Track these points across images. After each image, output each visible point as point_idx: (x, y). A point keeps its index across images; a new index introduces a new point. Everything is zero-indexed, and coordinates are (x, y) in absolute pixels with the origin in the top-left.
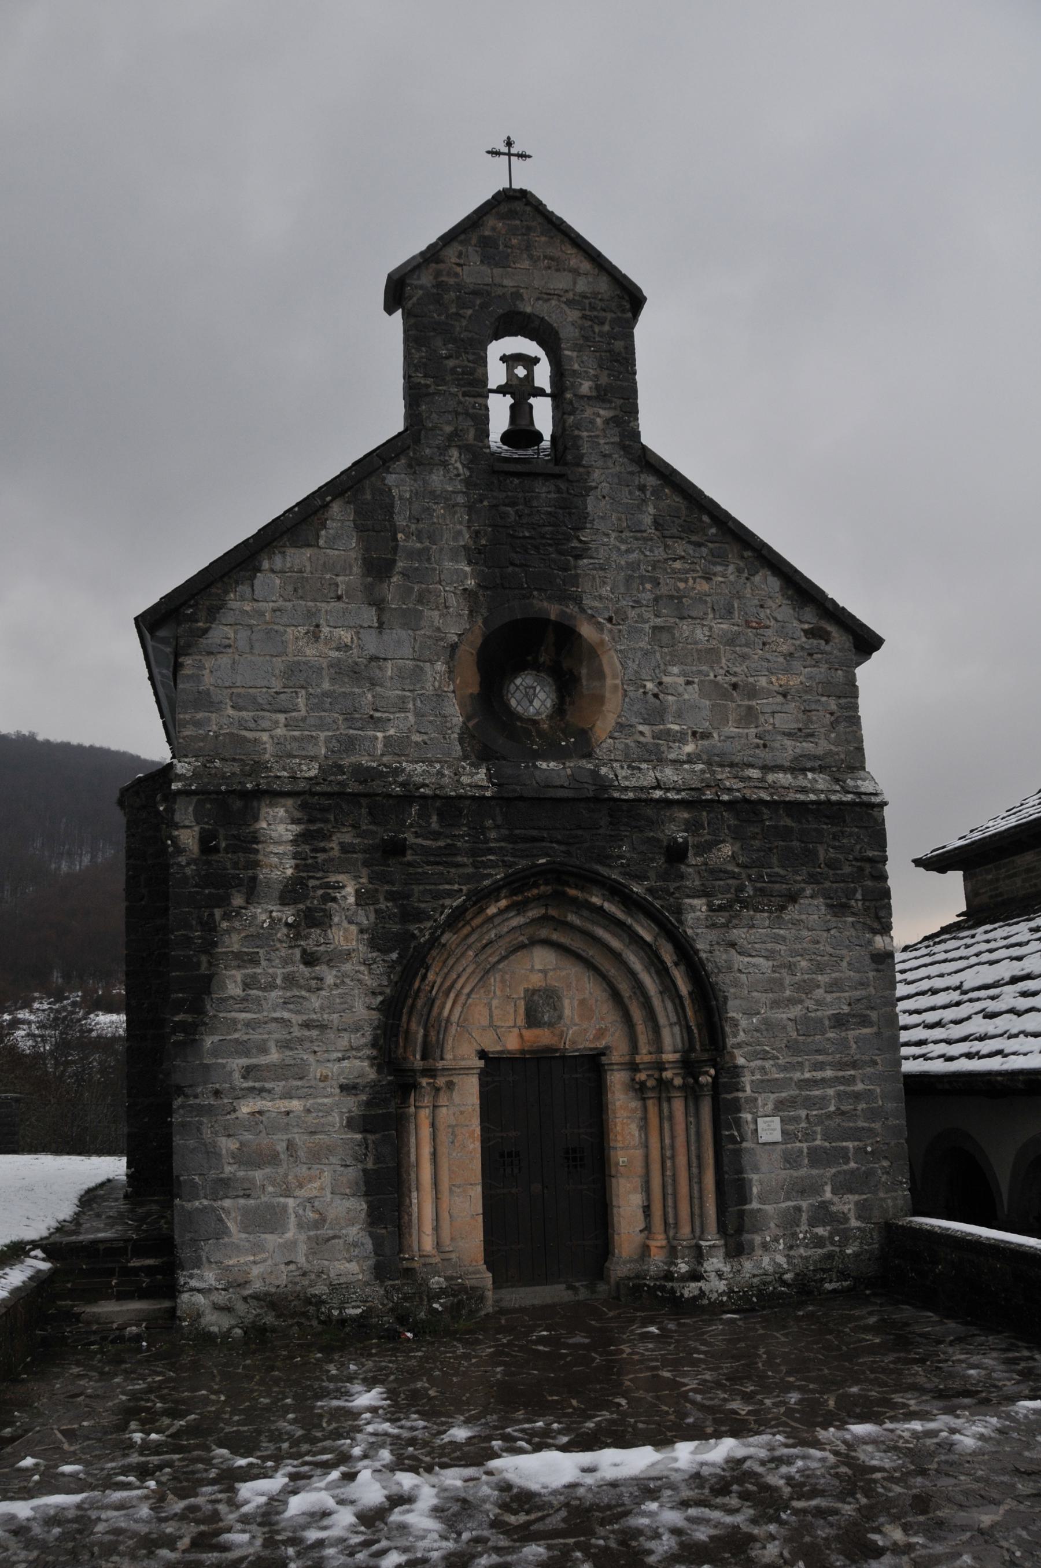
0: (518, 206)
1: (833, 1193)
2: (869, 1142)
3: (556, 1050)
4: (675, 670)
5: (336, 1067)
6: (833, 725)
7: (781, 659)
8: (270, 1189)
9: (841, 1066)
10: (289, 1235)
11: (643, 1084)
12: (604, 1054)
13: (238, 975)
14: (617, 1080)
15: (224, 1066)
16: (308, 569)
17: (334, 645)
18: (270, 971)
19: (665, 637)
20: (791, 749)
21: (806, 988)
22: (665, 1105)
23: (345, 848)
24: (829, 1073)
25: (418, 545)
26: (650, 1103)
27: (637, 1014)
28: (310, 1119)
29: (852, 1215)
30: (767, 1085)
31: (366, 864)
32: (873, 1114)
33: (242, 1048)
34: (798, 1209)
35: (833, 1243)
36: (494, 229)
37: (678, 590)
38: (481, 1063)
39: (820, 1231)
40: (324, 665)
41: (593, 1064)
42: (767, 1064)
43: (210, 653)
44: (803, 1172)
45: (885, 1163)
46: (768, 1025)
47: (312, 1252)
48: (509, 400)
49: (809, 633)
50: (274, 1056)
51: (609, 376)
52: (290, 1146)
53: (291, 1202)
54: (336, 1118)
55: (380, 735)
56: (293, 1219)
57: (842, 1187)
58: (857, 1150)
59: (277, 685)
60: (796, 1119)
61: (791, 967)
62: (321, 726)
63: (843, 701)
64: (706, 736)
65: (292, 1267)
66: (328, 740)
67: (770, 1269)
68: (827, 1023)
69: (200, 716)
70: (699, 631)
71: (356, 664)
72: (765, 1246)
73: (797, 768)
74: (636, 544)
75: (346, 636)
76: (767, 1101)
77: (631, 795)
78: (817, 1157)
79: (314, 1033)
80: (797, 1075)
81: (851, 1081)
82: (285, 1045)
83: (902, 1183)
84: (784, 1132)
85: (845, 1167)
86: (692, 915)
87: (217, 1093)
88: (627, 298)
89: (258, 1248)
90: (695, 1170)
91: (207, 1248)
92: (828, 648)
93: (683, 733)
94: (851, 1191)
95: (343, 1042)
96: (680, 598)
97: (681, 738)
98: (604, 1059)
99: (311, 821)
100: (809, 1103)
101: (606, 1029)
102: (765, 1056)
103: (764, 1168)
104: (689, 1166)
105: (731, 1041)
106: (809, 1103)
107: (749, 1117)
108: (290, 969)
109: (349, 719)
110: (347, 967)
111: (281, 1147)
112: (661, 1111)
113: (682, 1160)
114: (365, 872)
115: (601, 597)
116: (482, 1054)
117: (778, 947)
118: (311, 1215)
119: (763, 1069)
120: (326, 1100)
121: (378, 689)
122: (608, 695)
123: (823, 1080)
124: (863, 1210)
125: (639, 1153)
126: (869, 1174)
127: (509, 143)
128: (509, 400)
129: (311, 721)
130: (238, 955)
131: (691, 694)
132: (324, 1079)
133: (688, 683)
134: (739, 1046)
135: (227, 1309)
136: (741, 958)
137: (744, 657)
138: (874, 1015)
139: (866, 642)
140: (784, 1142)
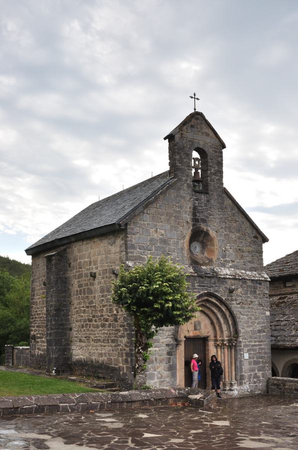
0: (199, 116)
4: (228, 245)
9: (259, 342)
10: (155, 380)
11: (218, 345)
21: (253, 323)
22: (223, 350)
24: (257, 343)
25: (178, 210)
26: (219, 350)
27: (217, 328)
30: (246, 346)
32: (265, 353)
34: (251, 374)
38: (185, 339)
39: (255, 380)
44: (251, 366)
47: (160, 385)
52: (156, 359)
54: (165, 352)
56: (156, 377)
58: (263, 361)
59: (148, 243)
60: (251, 354)
62: (158, 255)
64: (233, 261)
67: (246, 389)
69: (132, 250)
72: (245, 383)
75: (163, 232)
76: (246, 349)
77: (222, 277)
80: (251, 344)
81: (261, 345)
84: (249, 357)
90: (230, 365)
95: (167, 334)
97: (228, 262)
98: (209, 339)
100: (254, 350)
103: (245, 365)
104: (228, 364)
105: (240, 335)
106: (254, 350)
112: (221, 351)
113: (226, 363)
115: (215, 226)
118: (160, 376)
122: (215, 250)
123: (256, 345)
126: (264, 367)
127: (195, 95)
131: (231, 251)
137: (242, 242)
138: (266, 330)
139: (265, 240)
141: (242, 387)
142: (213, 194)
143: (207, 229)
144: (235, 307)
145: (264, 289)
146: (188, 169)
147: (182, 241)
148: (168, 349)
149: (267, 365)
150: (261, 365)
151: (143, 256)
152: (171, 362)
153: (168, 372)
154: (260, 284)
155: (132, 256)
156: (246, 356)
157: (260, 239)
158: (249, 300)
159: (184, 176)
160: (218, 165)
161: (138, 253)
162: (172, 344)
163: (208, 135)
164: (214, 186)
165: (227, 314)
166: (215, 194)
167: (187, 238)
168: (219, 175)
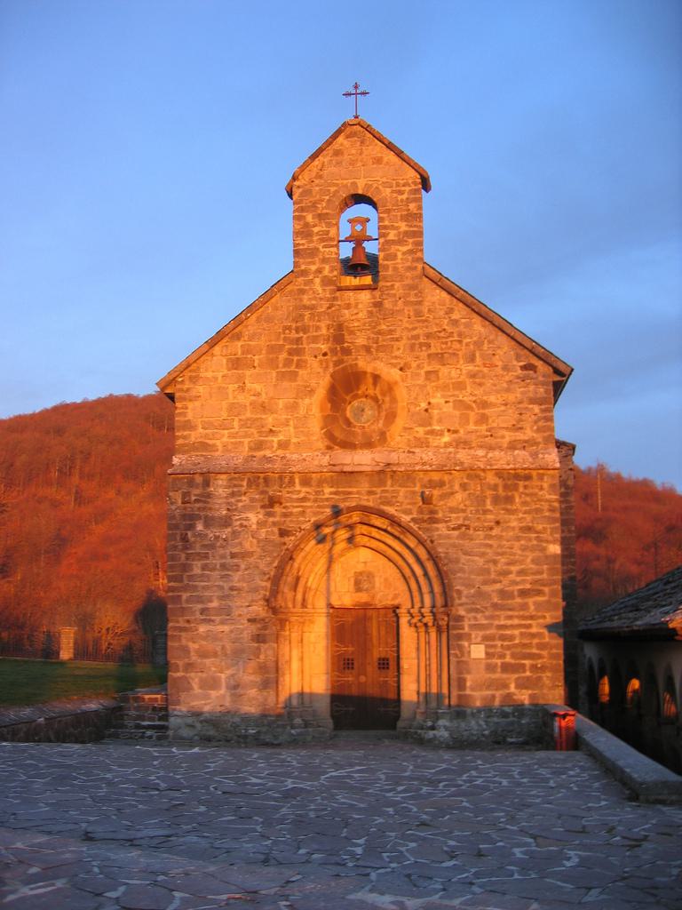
1: (517, 687)
2: (540, 661)
3: (371, 605)
5: (245, 610)
6: (536, 422)
7: (505, 385)
8: (213, 669)
12: (398, 608)
13: (199, 563)
16: (240, 353)
17: (252, 393)
18: (214, 562)
19: (433, 377)
20: (509, 436)
23: (252, 500)
24: (516, 622)
28: (233, 635)
31: (263, 507)
32: (541, 646)
33: (200, 600)
35: (514, 716)
36: (342, 145)
37: (442, 349)
40: (248, 404)
42: (479, 616)
43: (190, 400)
44: (497, 676)
45: (549, 674)
46: (480, 594)
48: (352, 245)
49: (524, 368)
50: (215, 604)
52: (223, 648)
53: (223, 676)
54: (246, 635)
55: (276, 440)
56: (224, 684)
59: (224, 415)
60: (495, 646)
61: (495, 562)
62: (245, 437)
63: (543, 407)
64: (456, 432)
65: (223, 708)
68: (516, 593)
69: (185, 433)
70: (453, 372)
71: (264, 402)
73: (512, 446)
74: (417, 325)
75: (258, 387)
76: (477, 635)
77: (403, 469)
78: (506, 668)
79: (235, 592)
80: (497, 622)
81: (529, 626)
82: (221, 598)
83: (558, 686)
85: (523, 675)
86: (437, 533)
87: (188, 621)
88: (419, 176)
89: (207, 697)
91: (183, 696)
92: (535, 376)
93: (442, 431)
94: (526, 688)
96: (442, 354)
97: (441, 434)
99: (235, 486)
100: (503, 638)
101: (399, 594)
102: (477, 611)
105: (457, 601)
106: (503, 638)
107: (466, 644)
113: (434, 666)
114: (262, 511)
115: (396, 357)
117: (488, 551)
118: (232, 682)
119: (475, 618)
120: (241, 626)
121: (275, 415)
122: (399, 412)
128: (352, 245)
129: (240, 434)
130: (198, 554)
131: (448, 408)
132: (240, 615)
133: (446, 402)
134: (461, 605)
135: (192, 726)
136: (464, 556)
137: (480, 385)
138: (546, 590)
140: (487, 659)
141: (463, 725)
143: (375, 369)
145: (541, 488)
146: (325, 247)
147: (307, 401)
148: (254, 628)
150: (528, 674)
152: (262, 657)
153: (252, 678)
154: (528, 478)
155: (183, 445)
156: (478, 651)
158: (490, 517)
159: (314, 263)
161: (201, 437)
162: (263, 620)
163: (379, 161)
164: (395, 269)
166: (397, 285)
167: (321, 392)
168: (411, 241)
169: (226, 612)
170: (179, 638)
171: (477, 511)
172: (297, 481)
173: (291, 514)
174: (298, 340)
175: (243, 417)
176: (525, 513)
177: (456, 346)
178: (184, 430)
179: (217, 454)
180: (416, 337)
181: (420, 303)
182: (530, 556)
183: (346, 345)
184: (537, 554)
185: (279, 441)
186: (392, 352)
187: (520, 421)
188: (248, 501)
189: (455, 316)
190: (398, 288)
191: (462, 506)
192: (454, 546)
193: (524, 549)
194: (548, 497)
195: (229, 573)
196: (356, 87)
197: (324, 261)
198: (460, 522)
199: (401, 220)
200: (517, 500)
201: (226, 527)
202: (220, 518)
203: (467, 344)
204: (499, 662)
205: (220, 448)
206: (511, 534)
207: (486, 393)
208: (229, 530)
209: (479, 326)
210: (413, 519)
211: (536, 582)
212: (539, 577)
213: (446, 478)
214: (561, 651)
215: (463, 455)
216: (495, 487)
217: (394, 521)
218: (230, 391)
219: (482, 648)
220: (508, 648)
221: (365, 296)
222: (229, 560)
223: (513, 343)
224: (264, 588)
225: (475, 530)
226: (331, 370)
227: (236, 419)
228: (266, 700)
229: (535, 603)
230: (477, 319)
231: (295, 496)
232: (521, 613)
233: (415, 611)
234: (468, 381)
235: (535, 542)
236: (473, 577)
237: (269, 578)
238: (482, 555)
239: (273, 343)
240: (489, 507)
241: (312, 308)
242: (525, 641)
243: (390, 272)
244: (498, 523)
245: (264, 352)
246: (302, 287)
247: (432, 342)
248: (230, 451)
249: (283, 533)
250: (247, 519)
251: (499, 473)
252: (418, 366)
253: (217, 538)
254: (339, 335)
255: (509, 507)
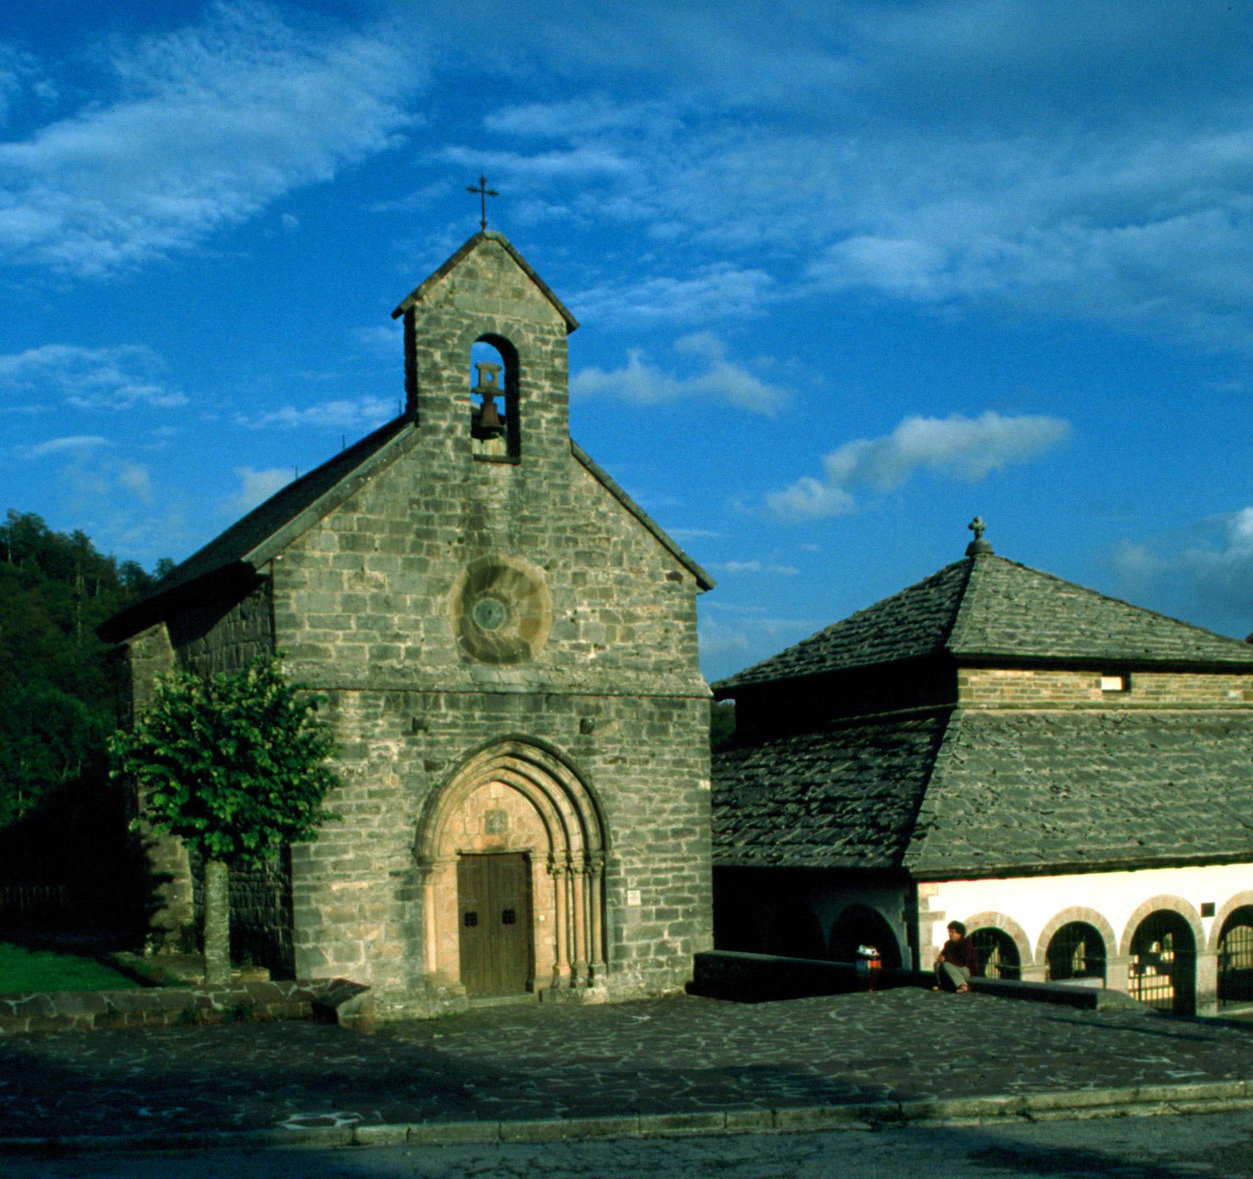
1: (670, 934)
6: (681, 641)
7: (651, 596)
9: (675, 860)
10: (362, 962)
14: (539, 867)
15: (321, 862)
16: (356, 528)
20: (655, 656)
21: (660, 812)
23: (392, 725)
27: (555, 827)
29: (679, 950)
31: (405, 734)
32: (693, 889)
33: (333, 851)
38: (458, 858)
39: (663, 958)
41: (525, 858)
42: (634, 859)
44: (652, 923)
46: (635, 835)
50: (350, 856)
51: (552, 386)
52: (361, 909)
55: (403, 646)
57: (675, 932)
59: (338, 609)
60: (650, 891)
61: (650, 799)
64: (602, 648)
66: (371, 649)
72: (630, 967)
73: (658, 669)
76: (632, 880)
78: (661, 915)
79: (375, 840)
80: (651, 866)
81: (682, 869)
82: (356, 847)
87: (319, 879)
96: (590, 553)
97: (586, 649)
98: (531, 855)
99: (370, 706)
100: (657, 882)
105: (614, 843)
106: (657, 882)
107: (622, 890)
108: (360, 802)
109: (384, 636)
110: (392, 800)
111: (355, 911)
113: (580, 917)
114: (404, 739)
115: (541, 553)
116: (460, 853)
119: (631, 862)
120: (382, 882)
122: (544, 619)
124: (686, 948)
125: (553, 912)
131: (595, 620)
134: (618, 847)
137: (627, 593)
138: (697, 829)
142: (535, 464)
144: (599, 768)
145: (694, 718)
146: (457, 398)
147: (440, 599)
148: (398, 883)
149: (699, 919)
150: (681, 919)
151: (321, 645)
152: (407, 917)
153: (396, 943)
154: (682, 706)
156: (634, 898)
157: (689, 579)
158: (647, 749)
160: (552, 380)
162: (406, 872)
164: (540, 441)
165: (576, 788)
166: (541, 461)
167: (456, 589)
168: (556, 406)
169: (363, 864)
170: (307, 900)
171: (634, 742)
172: (442, 701)
173: (438, 742)
174: (428, 520)
175: (363, 614)
176: (680, 744)
177: (604, 544)
178: (287, 627)
179: (331, 661)
180: (562, 529)
181: (566, 487)
182: (684, 792)
183: (484, 531)
184: (689, 790)
185: (407, 649)
186: (536, 546)
187: (665, 638)
188: (386, 725)
189: (603, 508)
190: (543, 466)
191: (618, 736)
192: (611, 781)
193: (677, 785)
194: (700, 727)
195: (368, 816)
196: (474, 190)
197: (457, 417)
198: (616, 754)
199: (546, 378)
200: (671, 730)
201: (362, 758)
202: (354, 747)
203: (615, 544)
204: (654, 908)
205: (334, 654)
206: (665, 768)
207: (633, 604)
208: (365, 762)
209: (627, 524)
210: (570, 751)
211: (687, 821)
212: (691, 815)
213: (602, 703)
214: (710, 894)
215: (613, 676)
216: (651, 716)
217: (549, 751)
218: (345, 578)
219: (638, 893)
220: (662, 892)
221: (506, 471)
222: (366, 801)
223: (660, 546)
224: (409, 834)
225: (632, 763)
226: (468, 561)
227: (354, 616)
228: (414, 968)
229: (687, 844)
230: (625, 514)
231: (441, 721)
232: (675, 855)
233: (559, 854)
234: (615, 587)
235: (687, 777)
236: (629, 816)
237: (415, 823)
238: (638, 791)
239: (399, 519)
240: (645, 738)
241: (443, 478)
242: (679, 885)
243: (533, 444)
244: (653, 755)
245: (387, 530)
246: (431, 449)
247: (580, 537)
248: (346, 658)
249: (430, 766)
250: (387, 748)
251: (656, 699)
252: (565, 566)
253: (351, 772)
254: (476, 517)
255: (663, 738)
